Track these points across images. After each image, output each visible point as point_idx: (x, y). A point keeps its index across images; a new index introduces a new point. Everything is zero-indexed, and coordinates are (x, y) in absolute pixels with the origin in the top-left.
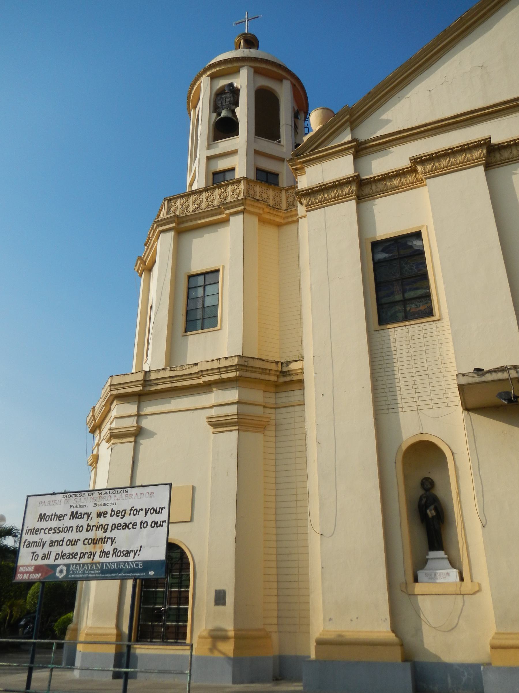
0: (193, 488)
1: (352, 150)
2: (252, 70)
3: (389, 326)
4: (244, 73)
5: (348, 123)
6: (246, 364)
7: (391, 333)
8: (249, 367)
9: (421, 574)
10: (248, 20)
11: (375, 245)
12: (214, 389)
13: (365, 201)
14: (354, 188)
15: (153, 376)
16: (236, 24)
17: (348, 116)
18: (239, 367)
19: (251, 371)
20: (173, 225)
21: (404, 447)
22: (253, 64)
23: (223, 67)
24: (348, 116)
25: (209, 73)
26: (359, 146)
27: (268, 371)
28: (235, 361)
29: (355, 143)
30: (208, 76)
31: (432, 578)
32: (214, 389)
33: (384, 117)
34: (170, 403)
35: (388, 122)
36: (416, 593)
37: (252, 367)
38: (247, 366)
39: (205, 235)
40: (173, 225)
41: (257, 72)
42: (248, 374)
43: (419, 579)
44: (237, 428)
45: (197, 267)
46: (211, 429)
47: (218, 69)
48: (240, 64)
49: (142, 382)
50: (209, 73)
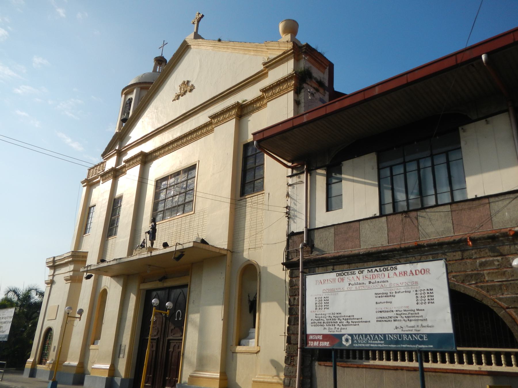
0: (58, 306)
1: (116, 154)
2: (140, 88)
3: (109, 239)
4: (135, 91)
5: (118, 140)
6: (75, 254)
7: (109, 242)
8: (76, 256)
9: (95, 342)
10: (163, 46)
11: (115, 199)
12: (69, 265)
13: (117, 178)
14: (112, 173)
15: (56, 259)
16: (159, 48)
17: (118, 137)
18: (72, 256)
19: (78, 257)
20: (86, 184)
21: (101, 291)
22: (139, 86)
23: (128, 90)
24: (118, 137)
25: (124, 92)
26: (119, 151)
27: (84, 257)
28: (70, 254)
29: (116, 151)
30: (124, 94)
31: (97, 344)
32: (69, 265)
33: (130, 136)
34: (61, 270)
35: (131, 137)
36: (90, 349)
37: (77, 256)
38: (75, 255)
39: (97, 187)
40: (86, 184)
41: (142, 88)
42: (76, 259)
43: (95, 343)
44: (69, 282)
45: (92, 204)
46: (65, 282)
47: (126, 91)
48: (134, 87)
49: (52, 262)
50: (124, 92)
